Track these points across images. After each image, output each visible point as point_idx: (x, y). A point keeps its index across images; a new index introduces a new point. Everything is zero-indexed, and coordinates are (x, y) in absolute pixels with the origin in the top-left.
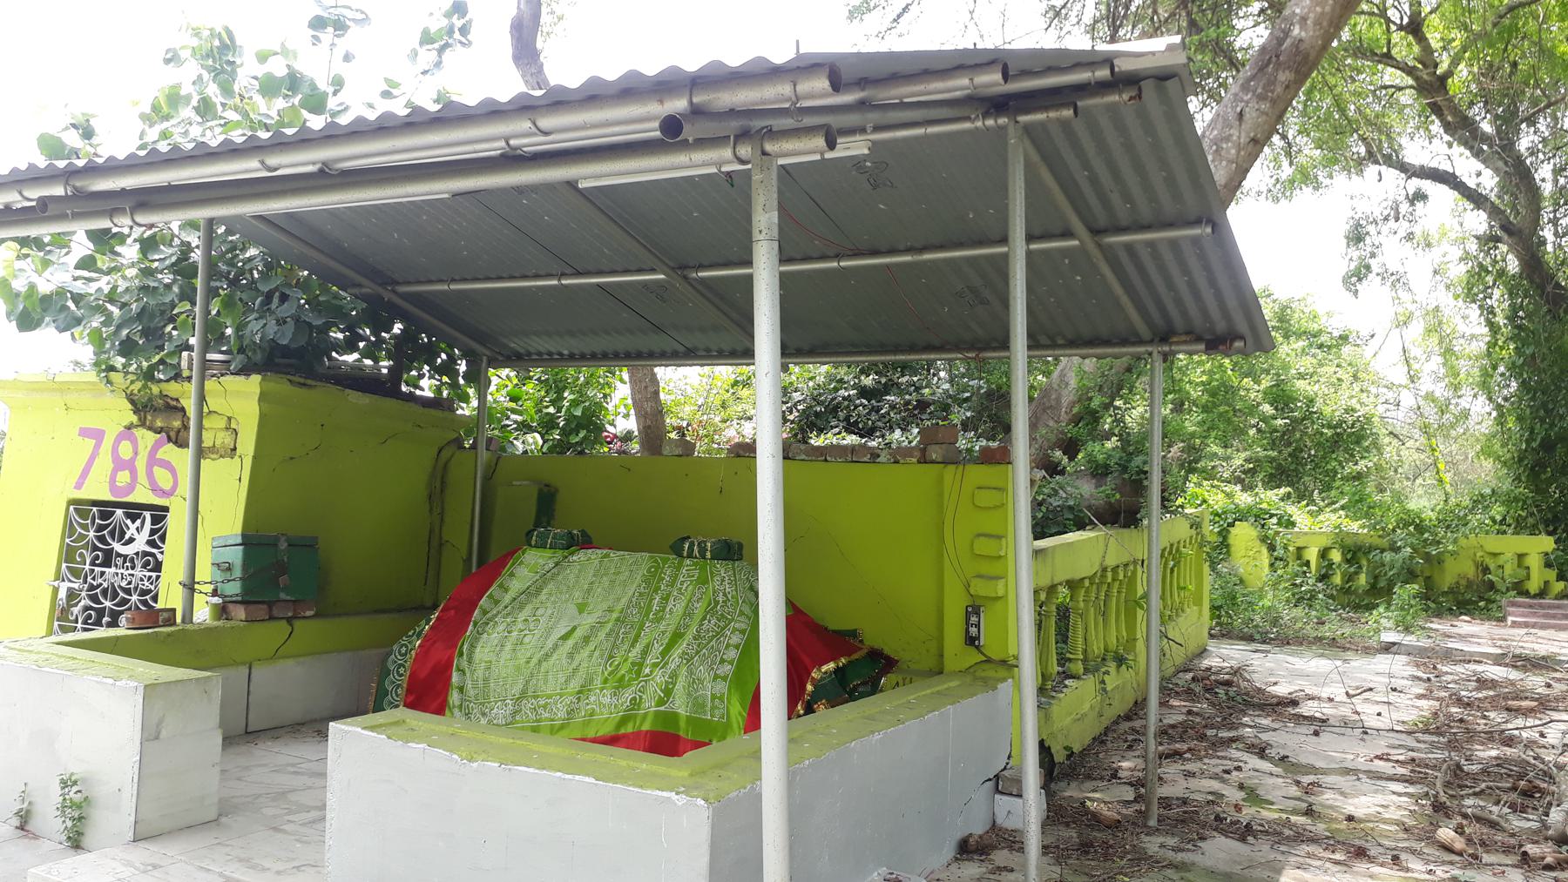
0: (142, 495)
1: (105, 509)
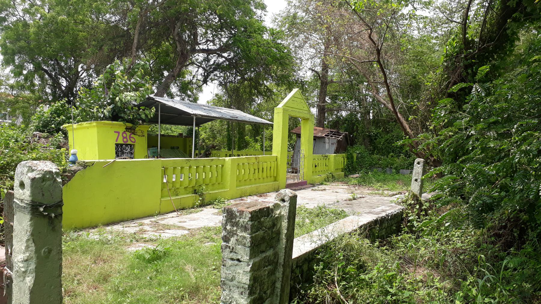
0: (129, 142)
1: (122, 145)
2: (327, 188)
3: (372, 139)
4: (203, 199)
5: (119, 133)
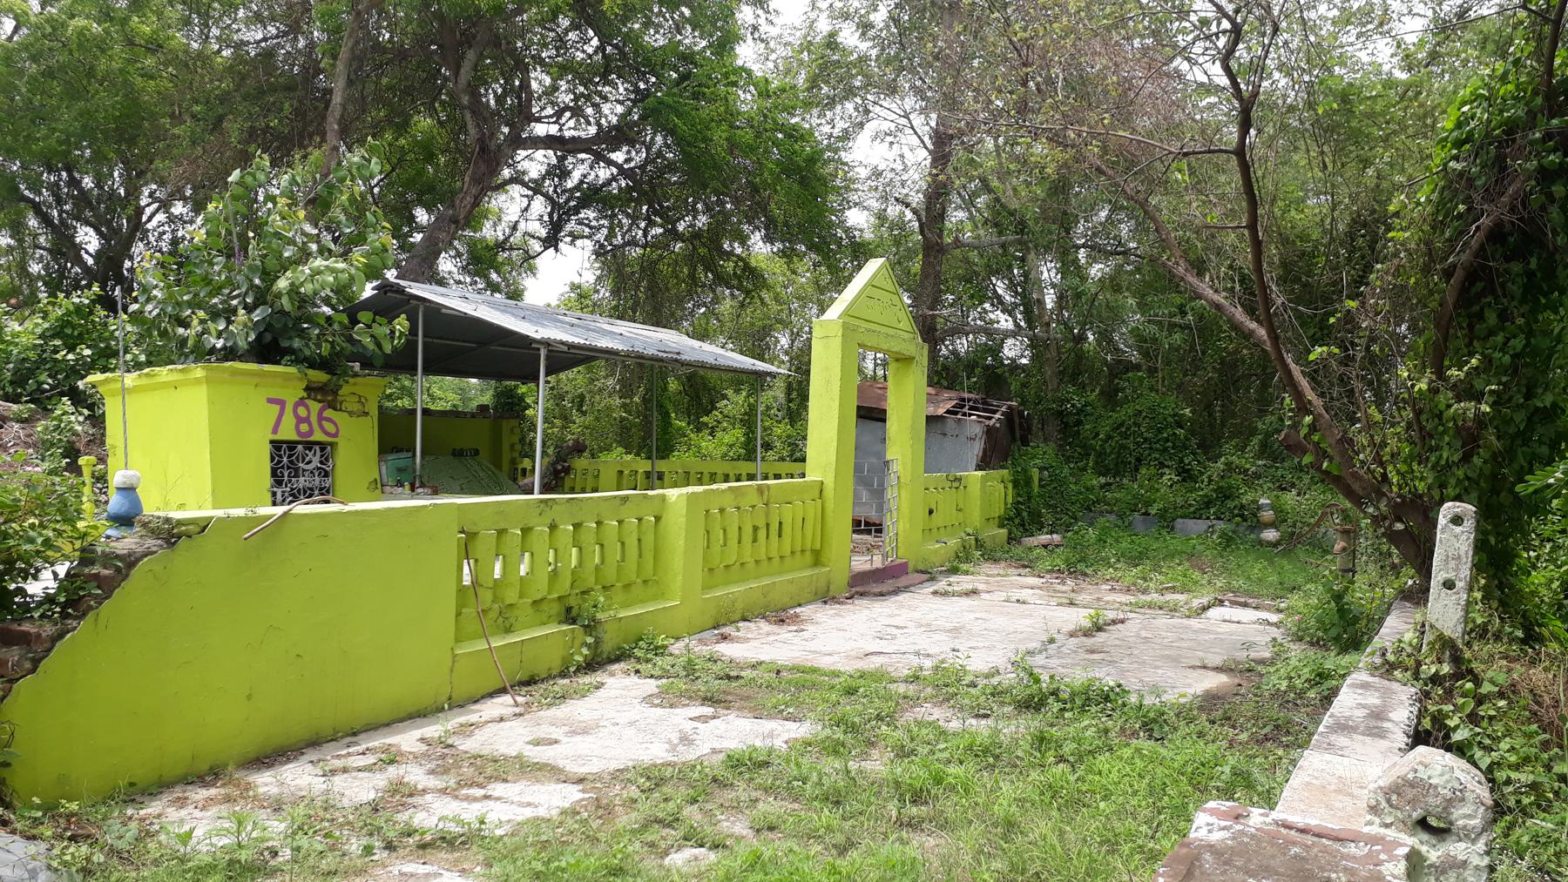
0: (318, 436)
1: (292, 445)
2: (981, 587)
3: (1066, 424)
4: (598, 642)
5: (281, 403)
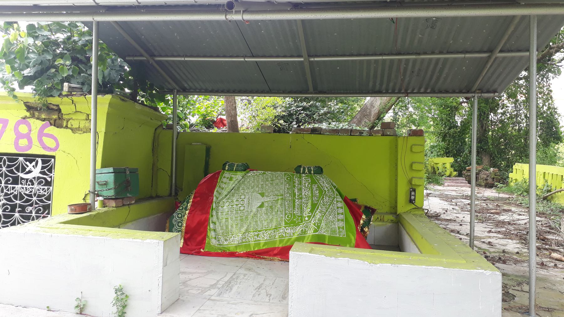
0: (36, 150)
